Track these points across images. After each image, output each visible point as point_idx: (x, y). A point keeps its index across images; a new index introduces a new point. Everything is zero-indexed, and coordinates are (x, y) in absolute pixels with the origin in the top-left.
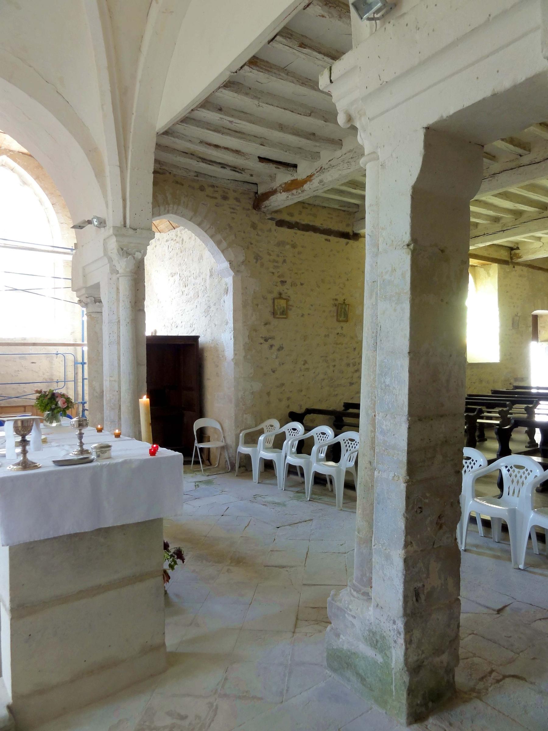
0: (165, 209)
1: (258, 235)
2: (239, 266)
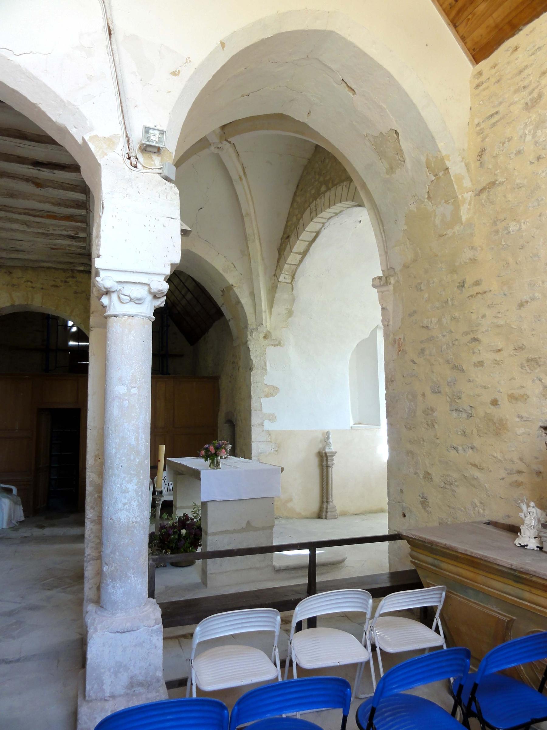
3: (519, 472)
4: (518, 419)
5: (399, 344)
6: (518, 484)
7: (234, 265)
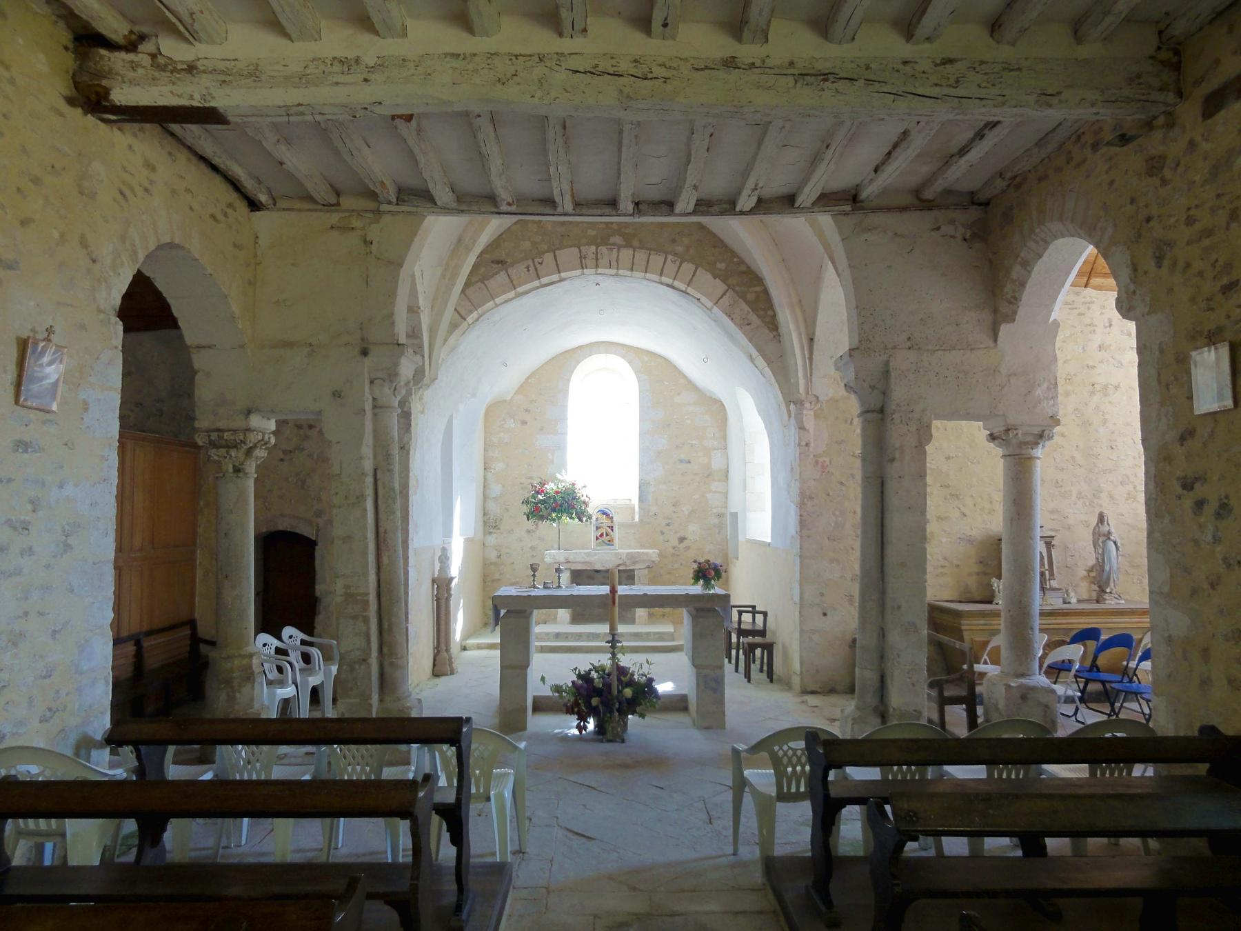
0: (1037, 242)
1: (1164, 182)
2: (1134, 292)
3: (943, 567)
4: (943, 533)
5: (823, 466)
6: (943, 574)
7: (422, 275)
